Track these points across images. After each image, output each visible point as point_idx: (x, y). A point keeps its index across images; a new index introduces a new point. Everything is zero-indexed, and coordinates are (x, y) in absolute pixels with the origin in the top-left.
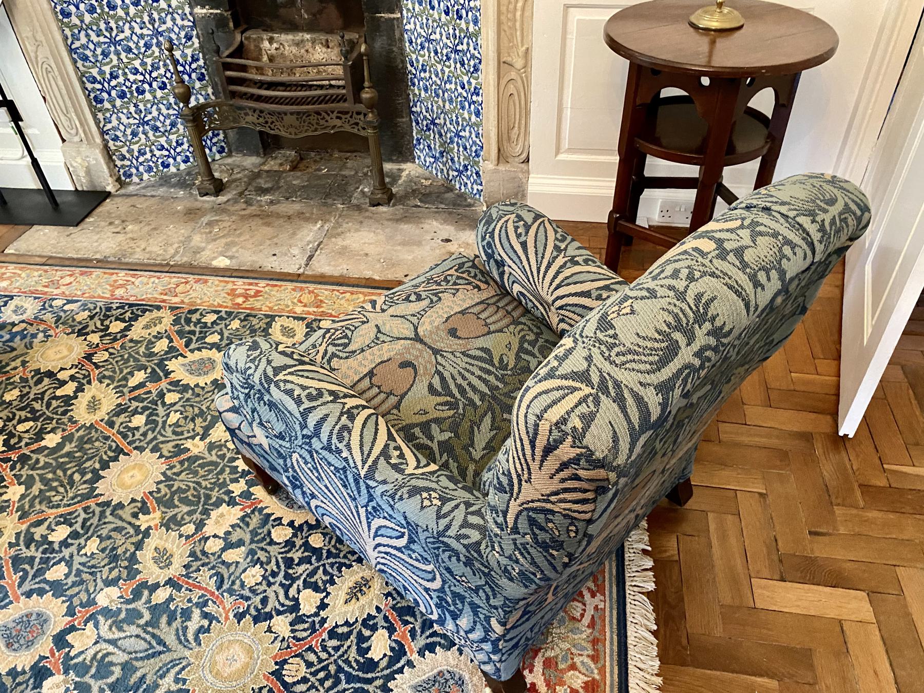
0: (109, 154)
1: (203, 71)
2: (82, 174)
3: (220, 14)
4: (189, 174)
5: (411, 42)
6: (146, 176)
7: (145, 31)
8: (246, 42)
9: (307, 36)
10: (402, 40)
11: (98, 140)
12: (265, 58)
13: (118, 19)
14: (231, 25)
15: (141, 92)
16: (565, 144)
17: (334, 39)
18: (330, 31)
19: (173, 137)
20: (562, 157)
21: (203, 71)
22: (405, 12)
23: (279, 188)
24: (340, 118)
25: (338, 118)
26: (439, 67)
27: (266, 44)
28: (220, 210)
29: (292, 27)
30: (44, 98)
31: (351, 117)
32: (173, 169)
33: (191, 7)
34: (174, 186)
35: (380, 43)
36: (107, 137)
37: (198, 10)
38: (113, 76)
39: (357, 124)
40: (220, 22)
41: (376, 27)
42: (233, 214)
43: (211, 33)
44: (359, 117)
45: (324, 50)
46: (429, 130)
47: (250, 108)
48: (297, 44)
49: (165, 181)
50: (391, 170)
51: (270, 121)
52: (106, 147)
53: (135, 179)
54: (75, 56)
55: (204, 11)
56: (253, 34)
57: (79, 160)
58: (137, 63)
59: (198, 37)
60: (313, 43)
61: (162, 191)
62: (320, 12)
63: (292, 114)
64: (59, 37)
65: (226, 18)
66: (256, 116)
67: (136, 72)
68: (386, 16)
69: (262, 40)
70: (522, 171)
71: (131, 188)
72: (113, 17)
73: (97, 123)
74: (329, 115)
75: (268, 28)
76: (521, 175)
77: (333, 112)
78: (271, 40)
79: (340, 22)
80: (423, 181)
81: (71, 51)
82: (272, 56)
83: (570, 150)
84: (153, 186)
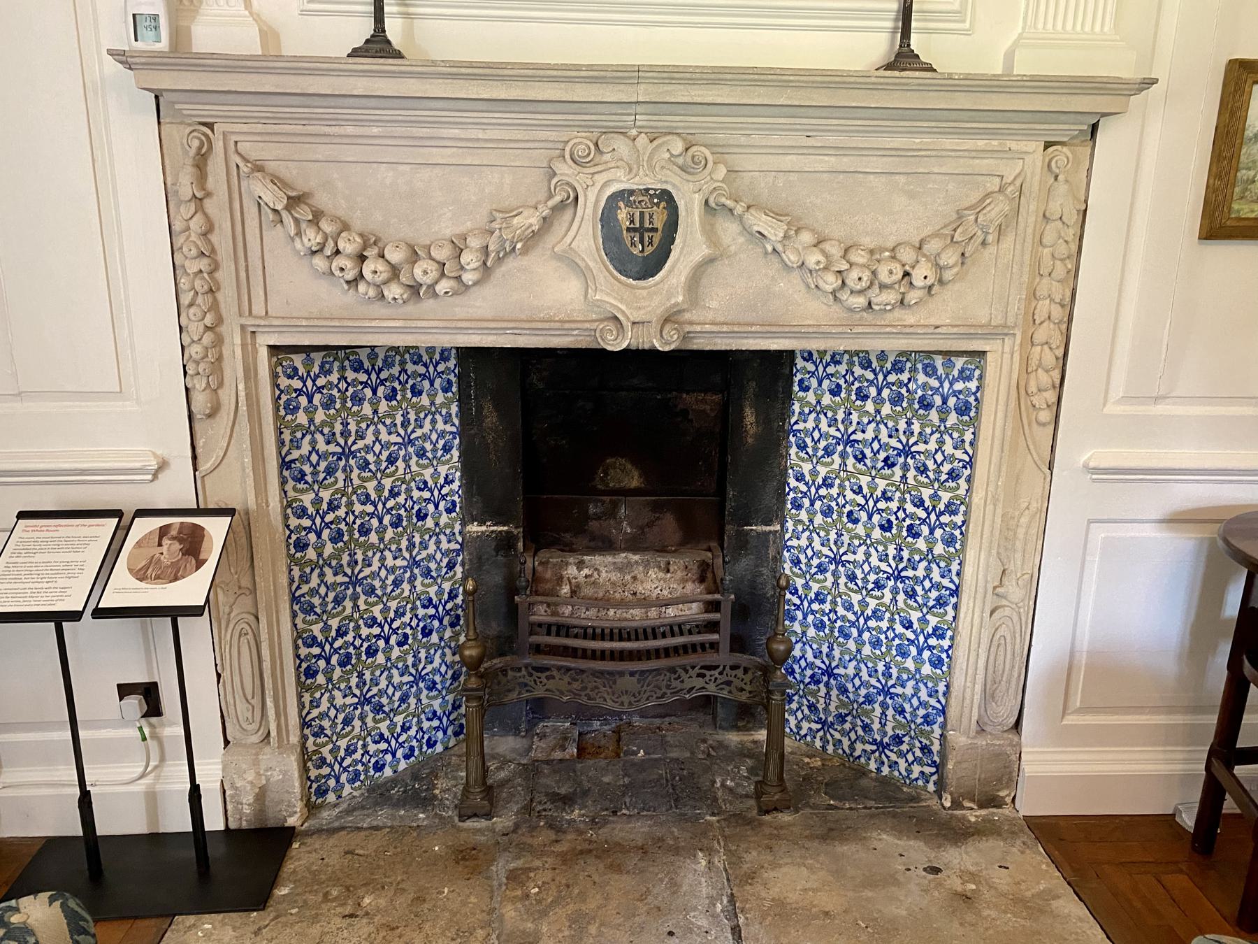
0: (305, 757)
1: (460, 612)
2: (248, 799)
3: (507, 532)
4: (415, 777)
5: (797, 562)
6: (347, 790)
7: (399, 562)
8: (540, 569)
9: (636, 557)
10: (778, 558)
11: (295, 739)
12: (566, 590)
13: (367, 547)
14: (520, 545)
15: (372, 652)
16: (1077, 701)
17: (677, 563)
18: (663, 550)
19: (399, 719)
20: (1070, 720)
21: (460, 612)
22: (790, 525)
23: (586, 793)
24: (703, 676)
25: (700, 675)
26: (856, 598)
27: (572, 571)
28: (507, 841)
29: (606, 545)
30: (219, 676)
31: (721, 673)
32: (388, 772)
33: (464, 524)
34: (399, 804)
35: (744, 565)
36: (307, 731)
37: (474, 528)
38: (341, 633)
39: (729, 683)
40: (505, 543)
41: (743, 542)
42: (543, 854)
43: (479, 556)
44: (734, 672)
45: (661, 575)
46: (818, 682)
47: (559, 668)
48: (621, 569)
49: (379, 795)
50: (741, 743)
51: (590, 686)
52: (304, 746)
53: (331, 797)
54: (296, 607)
55: (484, 528)
56: (544, 554)
57: (250, 776)
58: (376, 611)
59: (463, 564)
60: (645, 567)
61: (382, 816)
62: (650, 525)
63: (632, 674)
64: (284, 581)
65: (516, 538)
66: (567, 679)
67: (373, 622)
68: (759, 528)
69: (567, 564)
70: (1011, 745)
71: (325, 814)
72: (361, 545)
73: (301, 706)
74: (687, 672)
75: (570, 549)
76: (1009, 750)
77: (693, 668)
78: (580, 565)
79: (677, 537)
80: (806, 760)
81: (294, 599)
82: (578, 586)
83: (1085, 710)
84: (363, 808)
